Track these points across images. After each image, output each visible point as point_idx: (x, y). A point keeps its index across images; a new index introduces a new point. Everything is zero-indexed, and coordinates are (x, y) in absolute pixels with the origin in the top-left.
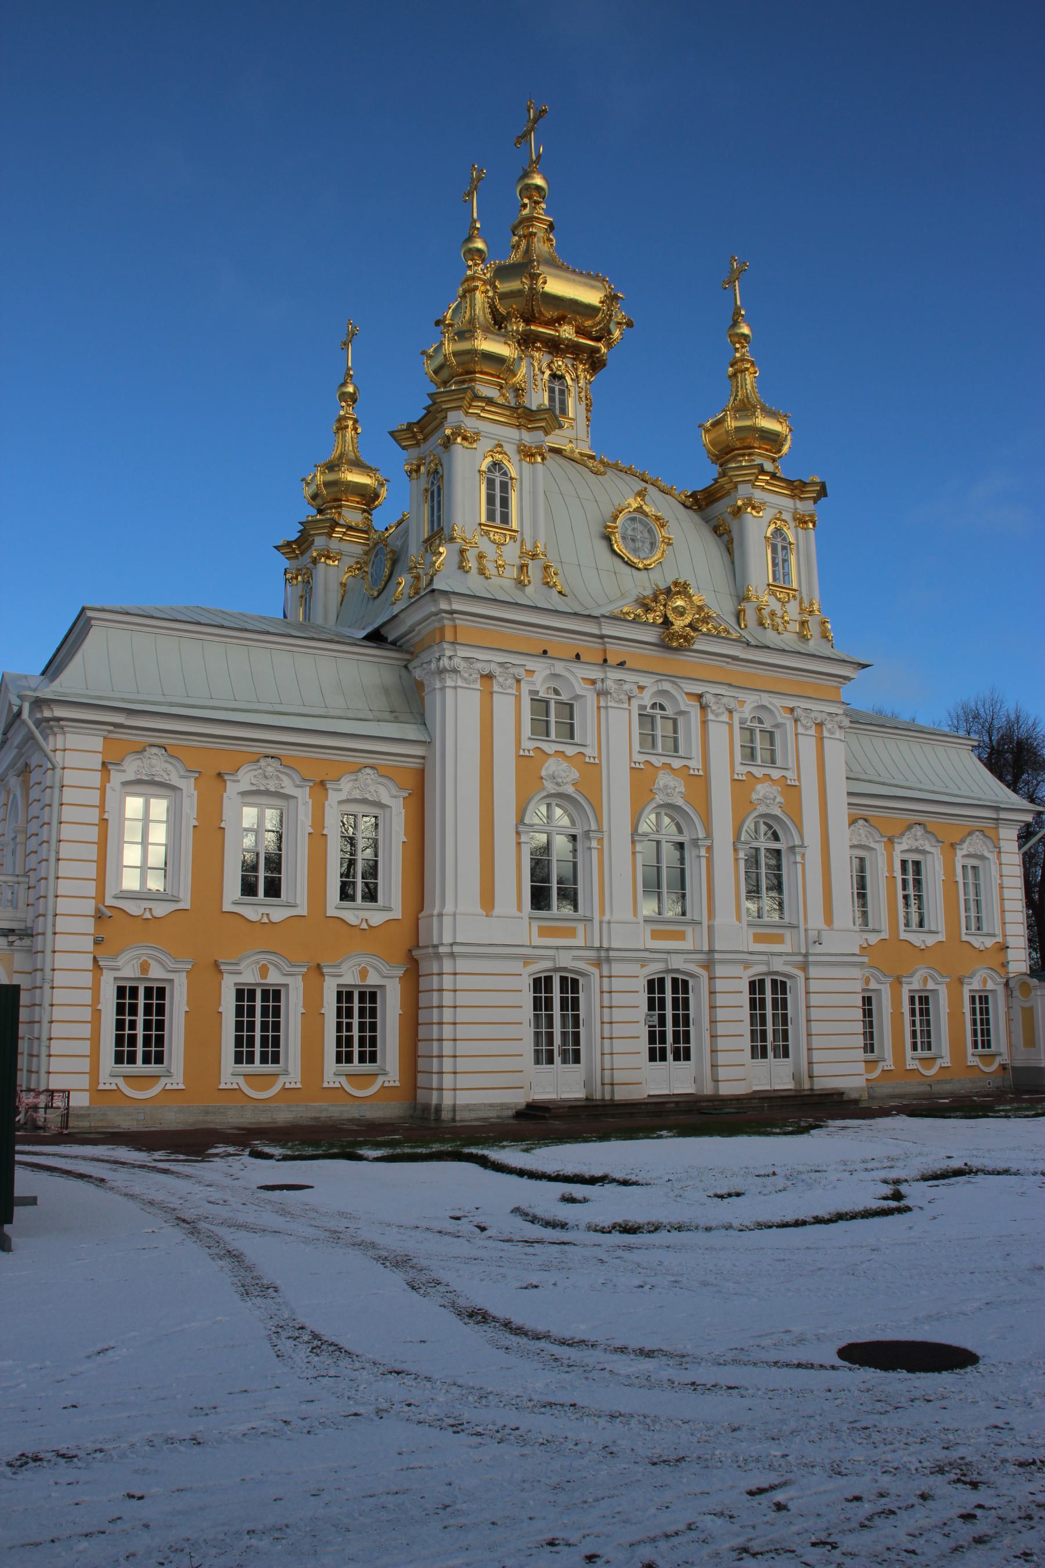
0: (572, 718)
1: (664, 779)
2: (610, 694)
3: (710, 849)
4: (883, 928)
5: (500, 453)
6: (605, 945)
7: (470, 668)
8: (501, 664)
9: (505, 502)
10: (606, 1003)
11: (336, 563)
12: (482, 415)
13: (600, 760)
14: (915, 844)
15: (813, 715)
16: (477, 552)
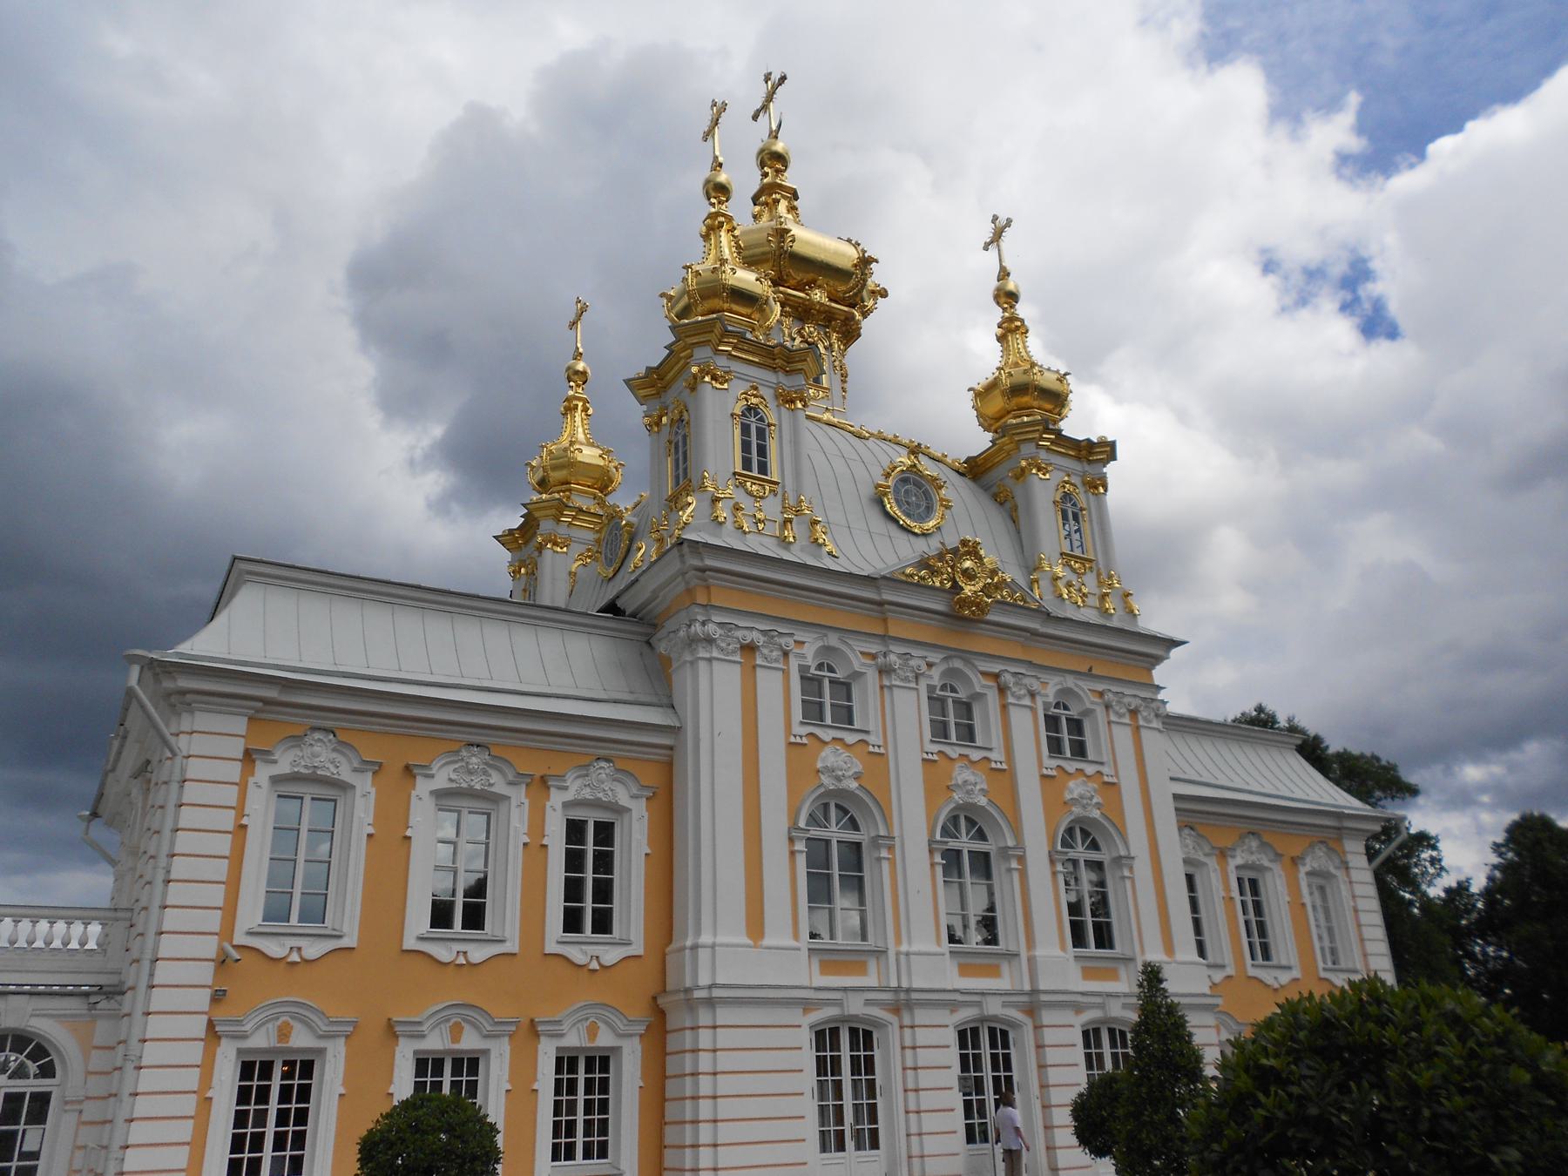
0: (849, 699)
1: (962, 775)
2: (895, 670)
3: (1022, 859)
4: (1226, 962)
5: (755, 396)
6: (905, 985)
7: (728, 636)
8: (764, 632)
9: (762, 451)
10: (909, 1064)
11: (565, 549)
12: (733, 353)
13: (886, 749)
14: (1253, 858)
15: (1126, 700)
16: (731, 505)
